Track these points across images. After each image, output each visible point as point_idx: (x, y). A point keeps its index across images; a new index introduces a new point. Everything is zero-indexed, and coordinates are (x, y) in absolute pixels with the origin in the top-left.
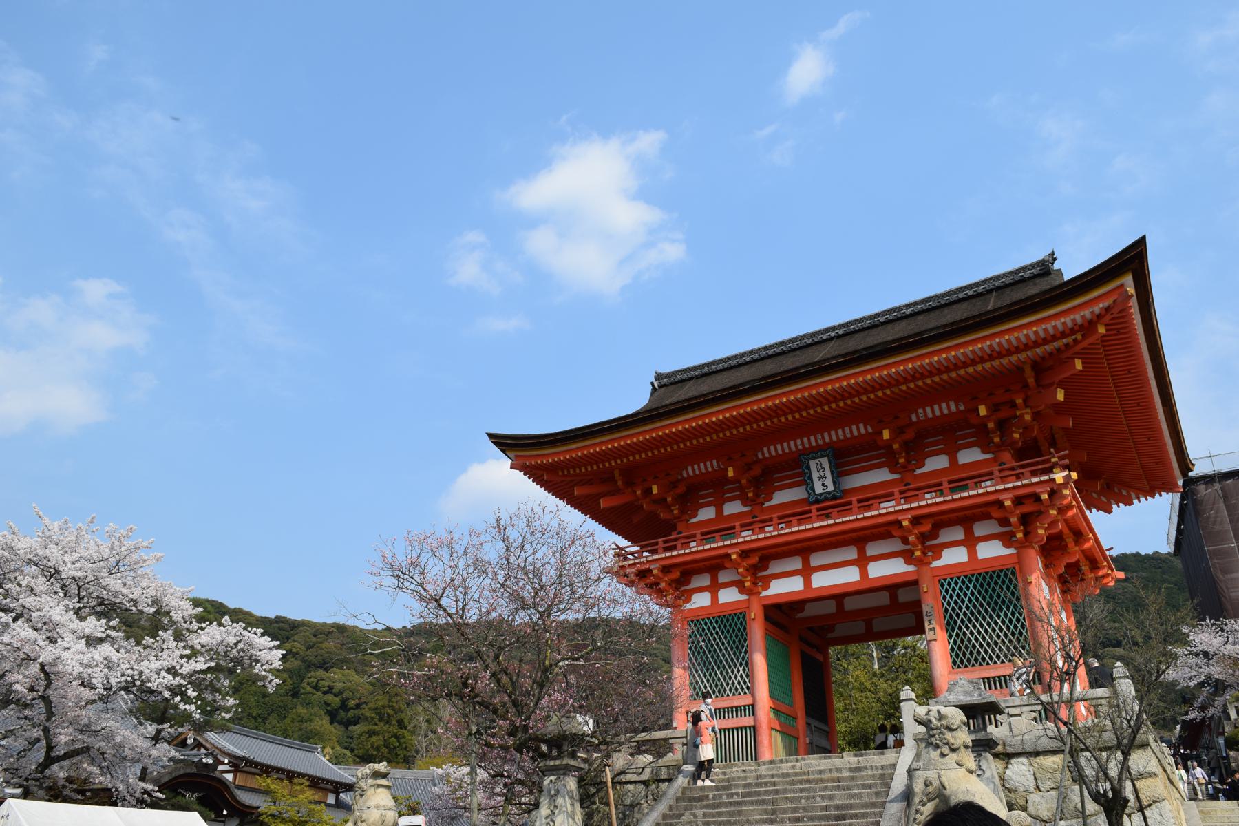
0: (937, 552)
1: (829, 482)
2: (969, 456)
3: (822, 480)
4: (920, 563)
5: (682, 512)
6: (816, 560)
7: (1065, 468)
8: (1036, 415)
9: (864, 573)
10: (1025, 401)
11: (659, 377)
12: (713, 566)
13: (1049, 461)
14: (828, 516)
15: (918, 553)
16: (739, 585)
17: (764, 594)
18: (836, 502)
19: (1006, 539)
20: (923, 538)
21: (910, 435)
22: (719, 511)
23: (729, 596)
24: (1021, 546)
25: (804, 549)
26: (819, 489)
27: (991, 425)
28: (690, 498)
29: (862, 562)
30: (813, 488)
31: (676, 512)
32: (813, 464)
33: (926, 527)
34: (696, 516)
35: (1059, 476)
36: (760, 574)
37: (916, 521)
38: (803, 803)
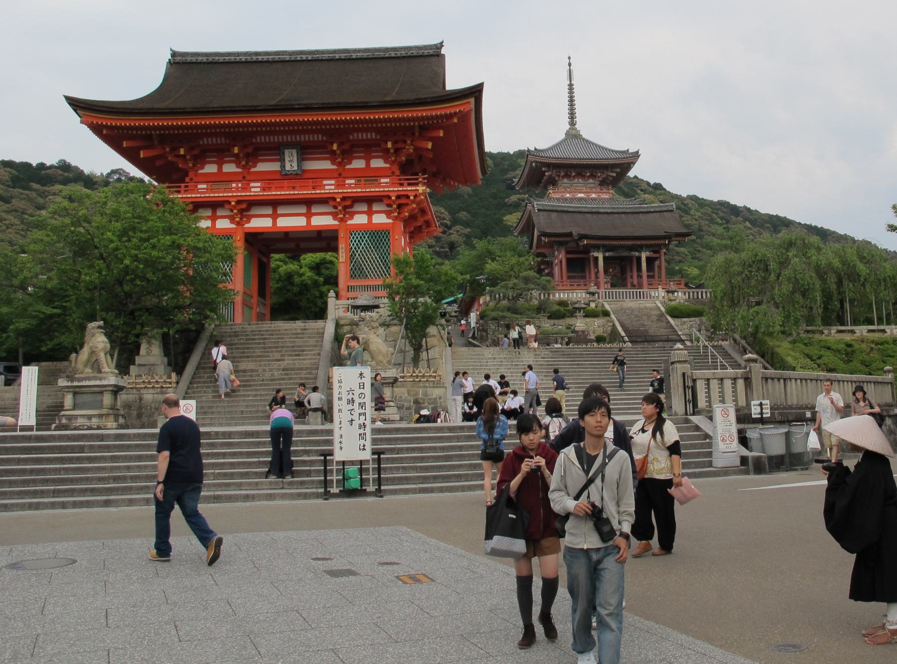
0: (352, 215)
1: (295, 165)
2: (377, 163)
3: (291, 163)
4: (342, 220)
5: (194, 165)
6: (280, 210)
7: (424, 184)
8: (414, 150)
9: (309, 222)
10: (412, 141)
11: (174, 54)
12: (215, 205)
13: (417, 179)
14: (294, 188)
15: (341, 216)
16: (232, 219)
17: (247, 226)
18: (299, 176)
19: (388, 214)
20: (345, 208)
21: (346, 147)
22: (220, 169)
23: (223, 224)
24: (395, 218)
25: (275, 204)
26: (288, 168)
27: (392, 151)
28: (200, 158)
29: (309, 215)
30: (284, 167)
31: (191, 165)
32: (287, 152)
33: (348, 203)
34: (203, 168)
35: (421, 189)
36: (245, 213)
37: (343, 199)
38: (280, 345)
